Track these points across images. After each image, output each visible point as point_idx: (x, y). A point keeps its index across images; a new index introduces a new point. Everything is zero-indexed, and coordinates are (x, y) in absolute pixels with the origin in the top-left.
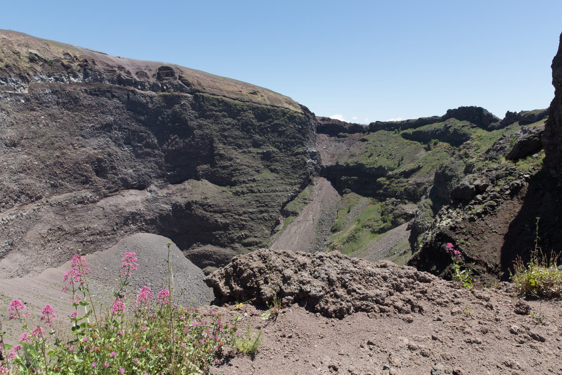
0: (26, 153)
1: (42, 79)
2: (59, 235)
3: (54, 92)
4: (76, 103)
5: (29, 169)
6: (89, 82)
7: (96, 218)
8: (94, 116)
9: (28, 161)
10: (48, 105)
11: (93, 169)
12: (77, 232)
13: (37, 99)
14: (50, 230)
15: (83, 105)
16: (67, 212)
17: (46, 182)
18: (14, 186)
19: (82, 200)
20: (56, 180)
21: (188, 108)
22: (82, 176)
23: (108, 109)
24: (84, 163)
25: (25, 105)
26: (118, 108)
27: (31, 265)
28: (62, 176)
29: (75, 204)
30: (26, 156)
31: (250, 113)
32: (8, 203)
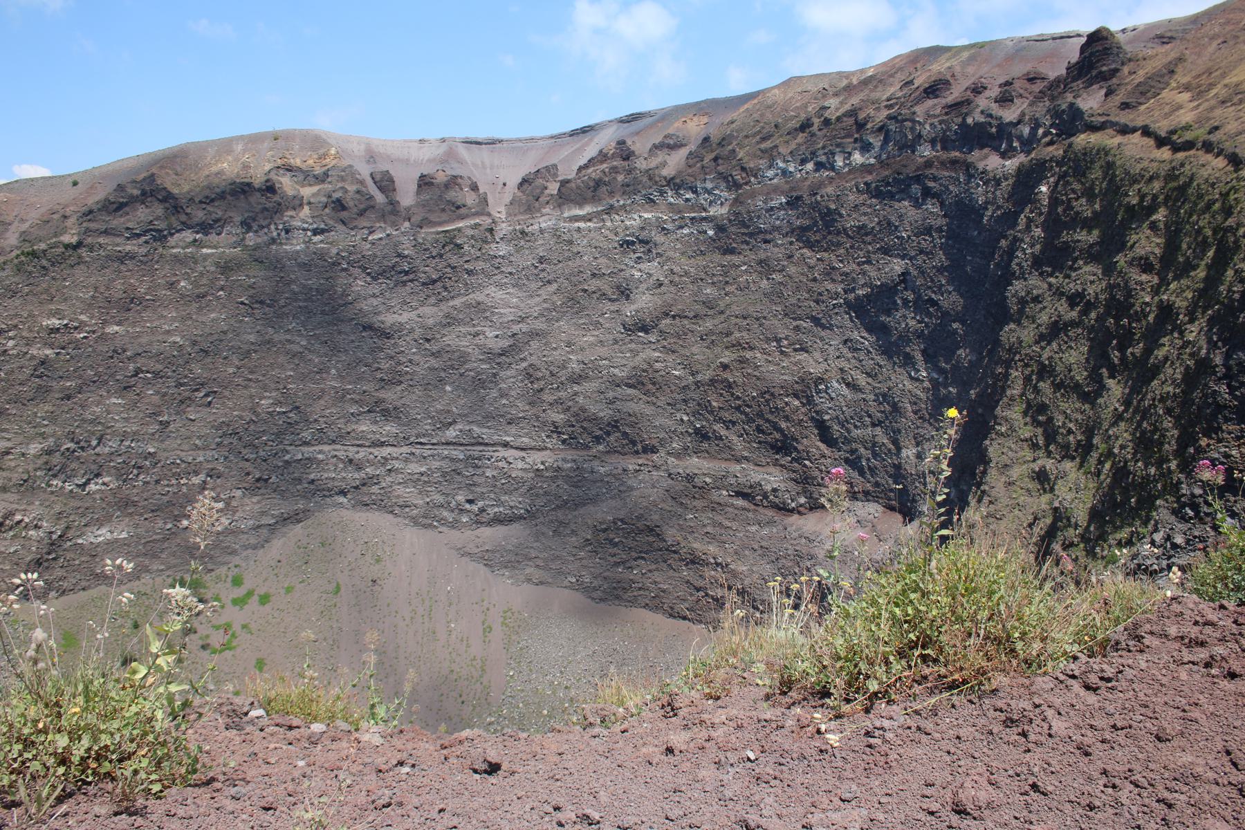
0: (664, 347)
1: (785, 172)
2: (650, 544)
3: (794, 202)
4: (828, 225)
5: (654, 384)
6: (888, 158)
7: (760, 552)
8: (864, 263)
9: (658, 365)
10: (768, 237)
11: (812, 419)
12: (694, 561)
13: (743, 224)
14: (622, 520)
15: (845, 230)
16: (696, 503)
17: (682, 420)
18: (602, 410)
19: (750, 491)
20: (708, 421)
21: (1041, 214)
22: (777, 428)
23: (898, 238)
24: (787, 396)
25: (714, 240)
26: (928, 231)
27: (530, 559)
28: (727, 415)
29: (730, 495)
30: (657, 354)
31: (1153, 226)
32: (576, 438)
